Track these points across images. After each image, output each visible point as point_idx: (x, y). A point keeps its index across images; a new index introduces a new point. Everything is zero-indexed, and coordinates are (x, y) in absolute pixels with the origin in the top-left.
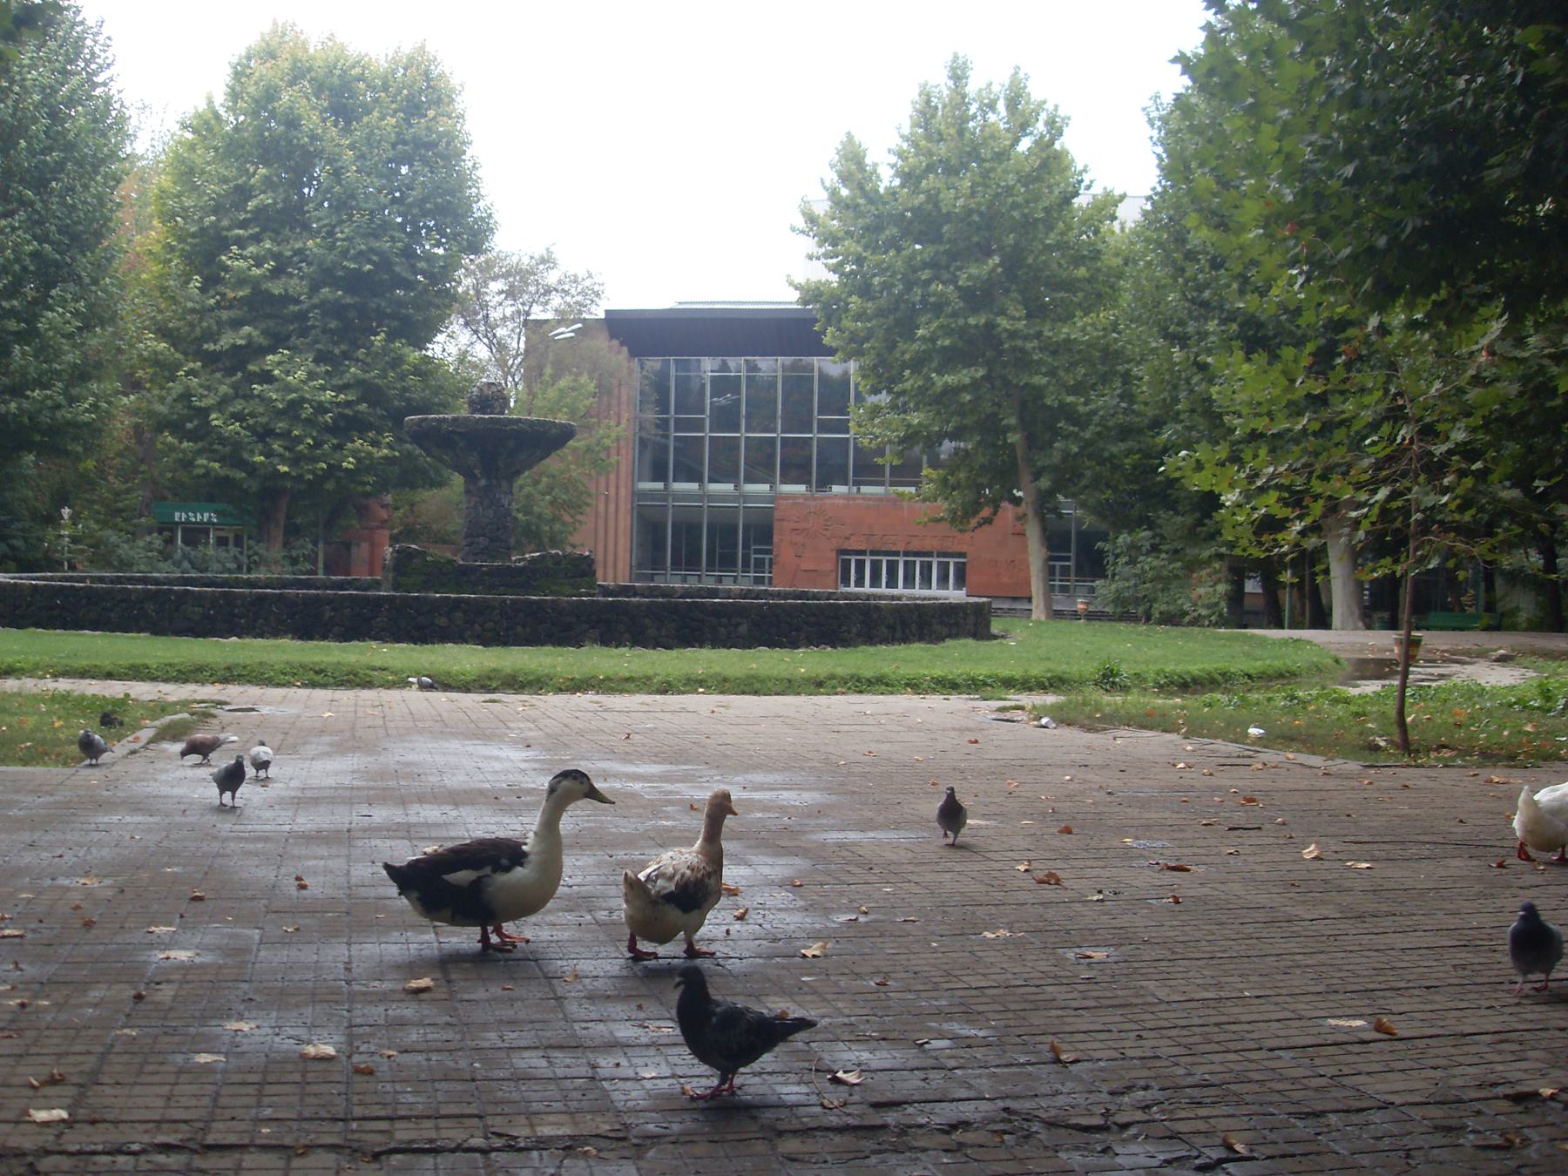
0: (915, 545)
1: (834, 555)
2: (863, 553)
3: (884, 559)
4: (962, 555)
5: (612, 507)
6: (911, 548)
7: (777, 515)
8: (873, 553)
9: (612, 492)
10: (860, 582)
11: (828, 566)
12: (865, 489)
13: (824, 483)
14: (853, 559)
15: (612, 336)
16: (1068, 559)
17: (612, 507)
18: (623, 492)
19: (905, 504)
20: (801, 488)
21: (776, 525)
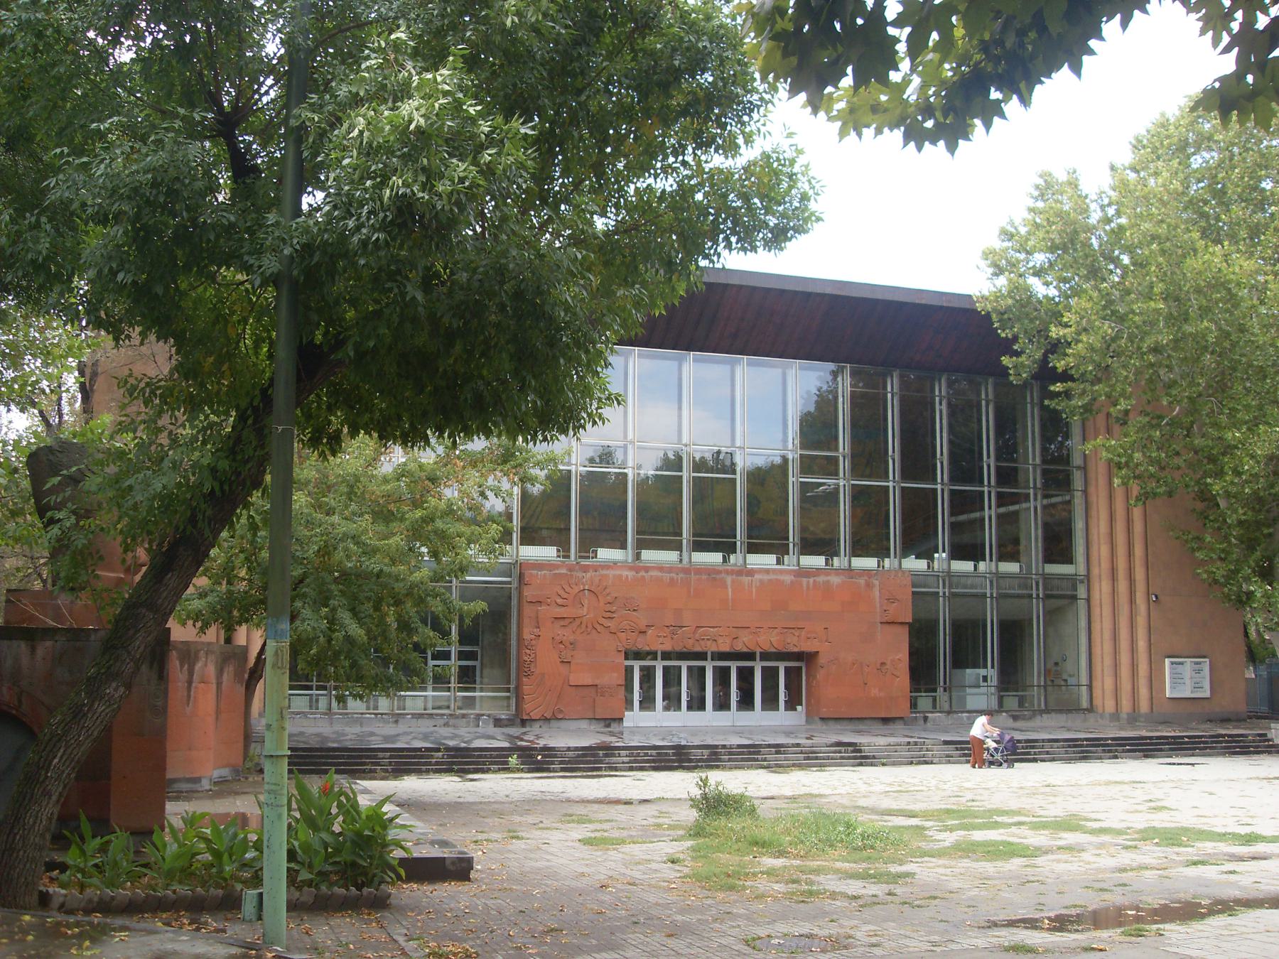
8: (666, 656)
11: (617, 678)
12: (648, 555)
13: (589, 543)
19: (729, 579)
20: (548, 553)
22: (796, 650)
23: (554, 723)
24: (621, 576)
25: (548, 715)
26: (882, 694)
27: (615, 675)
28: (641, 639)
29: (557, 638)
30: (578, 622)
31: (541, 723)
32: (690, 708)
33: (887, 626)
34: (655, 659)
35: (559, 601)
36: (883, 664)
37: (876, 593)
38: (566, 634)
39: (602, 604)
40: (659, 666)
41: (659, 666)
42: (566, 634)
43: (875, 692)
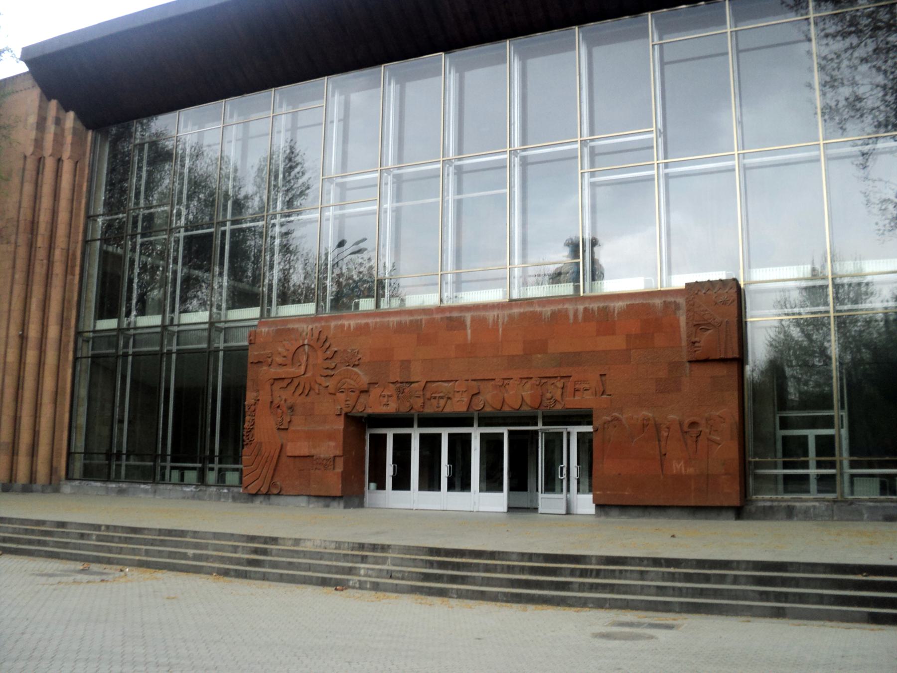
0: (488, 400)
1: (339, 425)
2: (405, 421)
3: (445, 433)
4: (584, 417)
5: (31, 356)
6: (478, 404)
7: (253, 355)
9: (33, 332)
10: (402, 482)
11: (330, 448)
14: (389, 434)
15: (48, 93)
16: (828, 422)
17: (31, 356)
18: (53, 331)
19: (468, 317)
21: (250, 374)
22: (559, 407)
23: (274, 499)
24: (343, 326)
25: (264, 490)
26: (691, 470)
27: (332, 444)
28: (363, 399)
29: (276, 402)
30: (296, 382)
31: (261, 498)
32: (451, 487)
33: (695, 367)
34: (411, 426)
35: (279, 359)
36: (693, 424)
37: (683, 320)
38: (283, 395)
39: (320, 361)
40: (415, 434)
41: (415, 434)
42: (283, 395)
43: (677, 467)
